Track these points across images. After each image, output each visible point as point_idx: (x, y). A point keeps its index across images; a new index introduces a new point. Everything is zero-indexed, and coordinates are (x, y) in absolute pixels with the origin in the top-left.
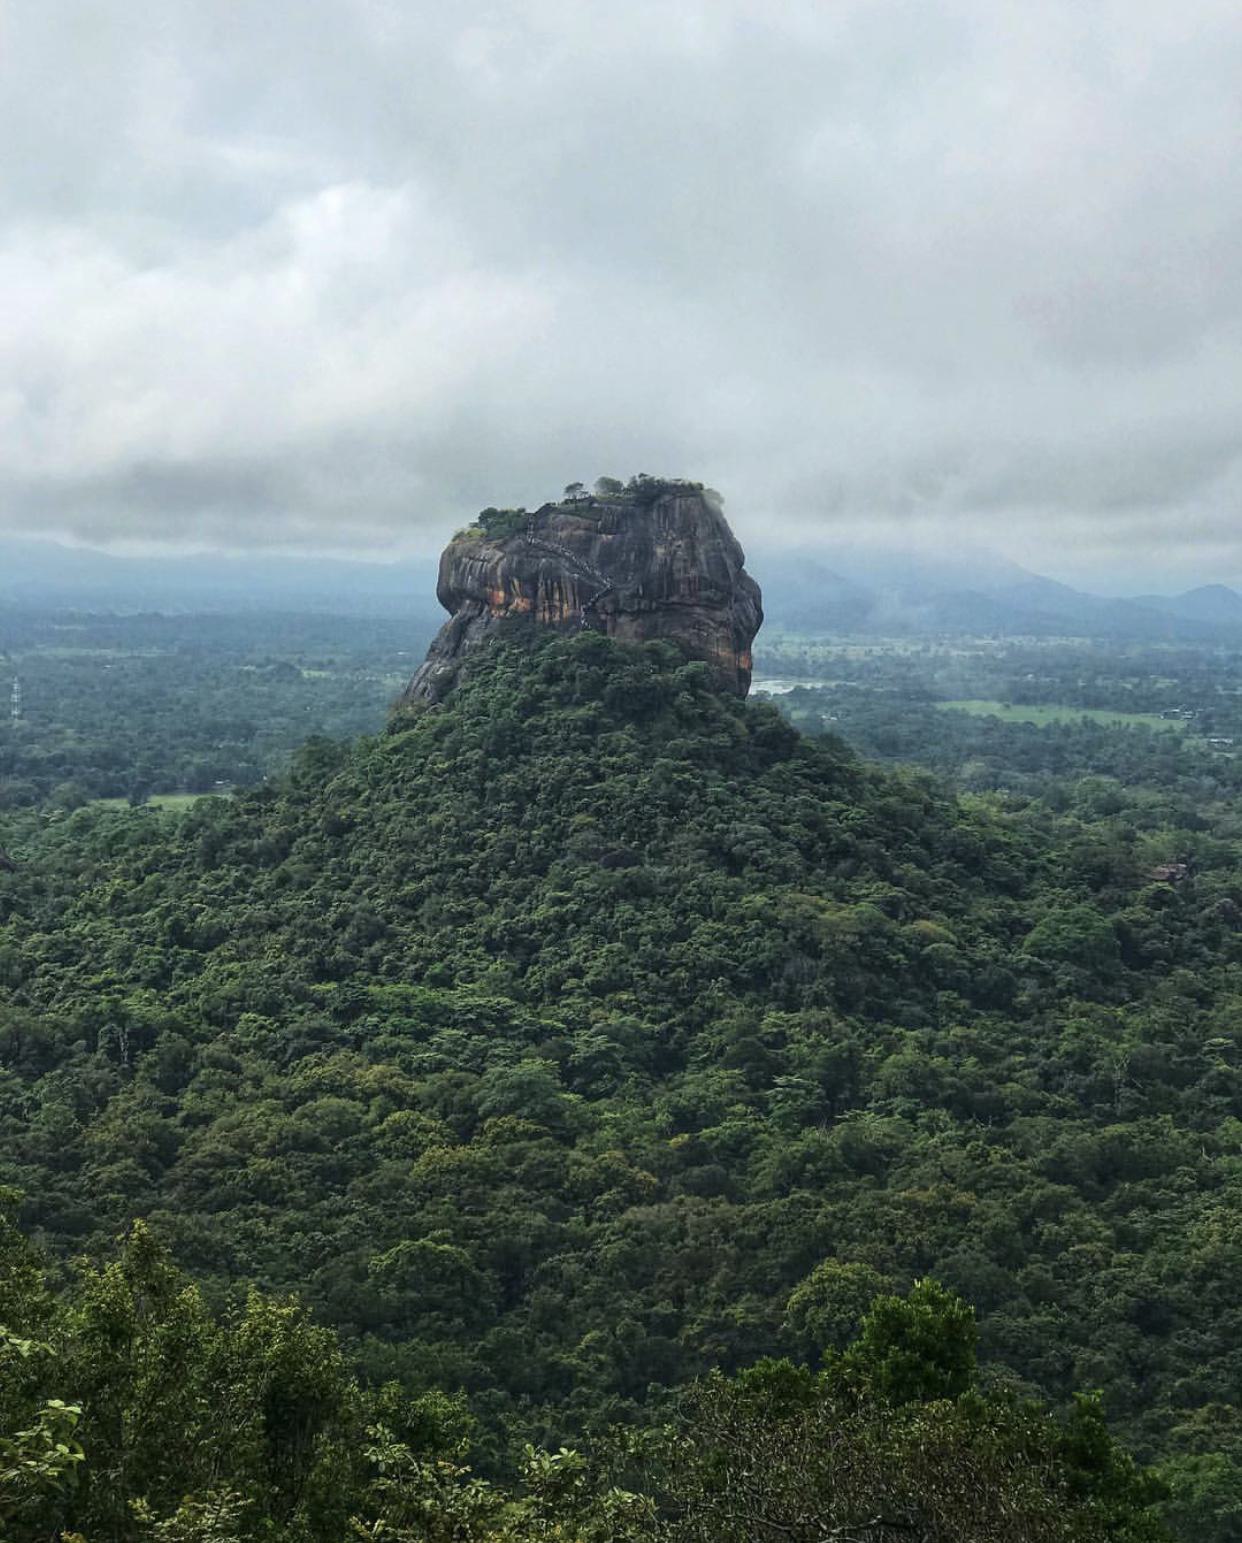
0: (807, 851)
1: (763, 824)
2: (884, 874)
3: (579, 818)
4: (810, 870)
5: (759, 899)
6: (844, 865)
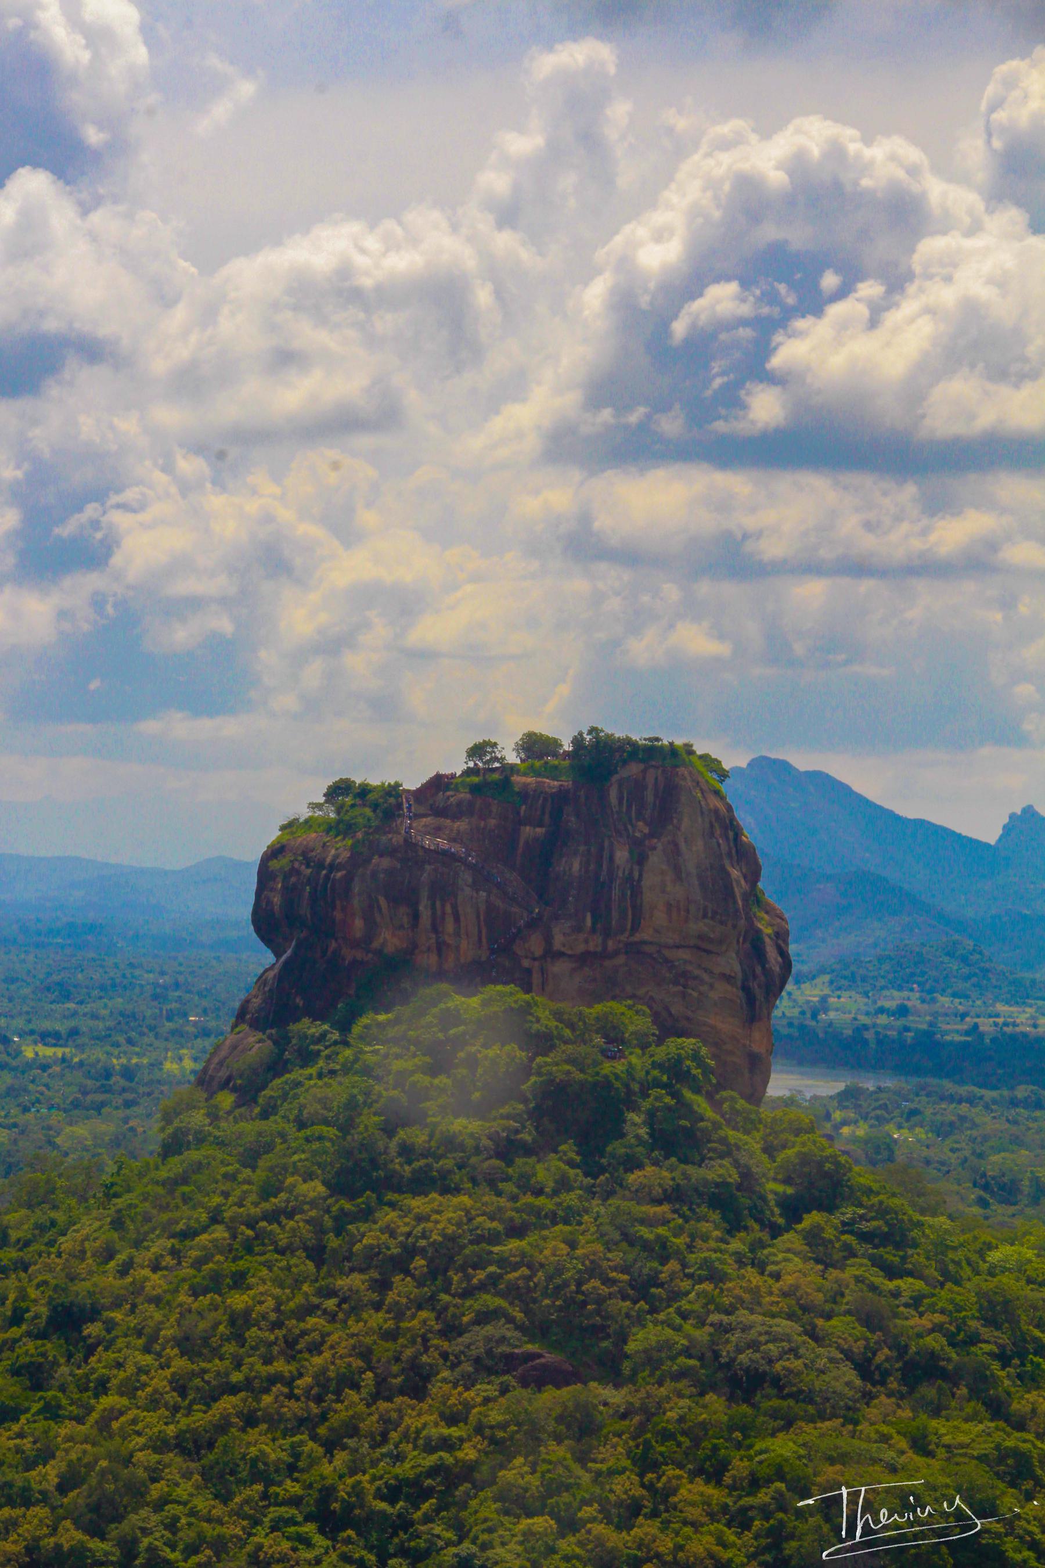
0: (864, 1367)
1: (790, 1316)
2: (997, 1409)
4: (868, 1397)
5: (782, 1447)
6: (929, 1391)
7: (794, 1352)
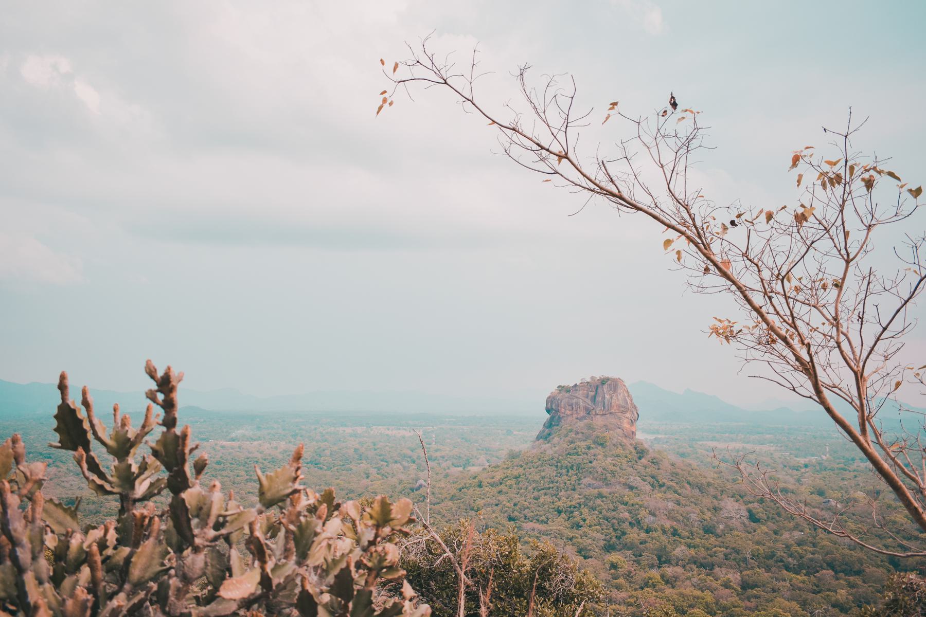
0: (652, 485)
6: (663, 489)
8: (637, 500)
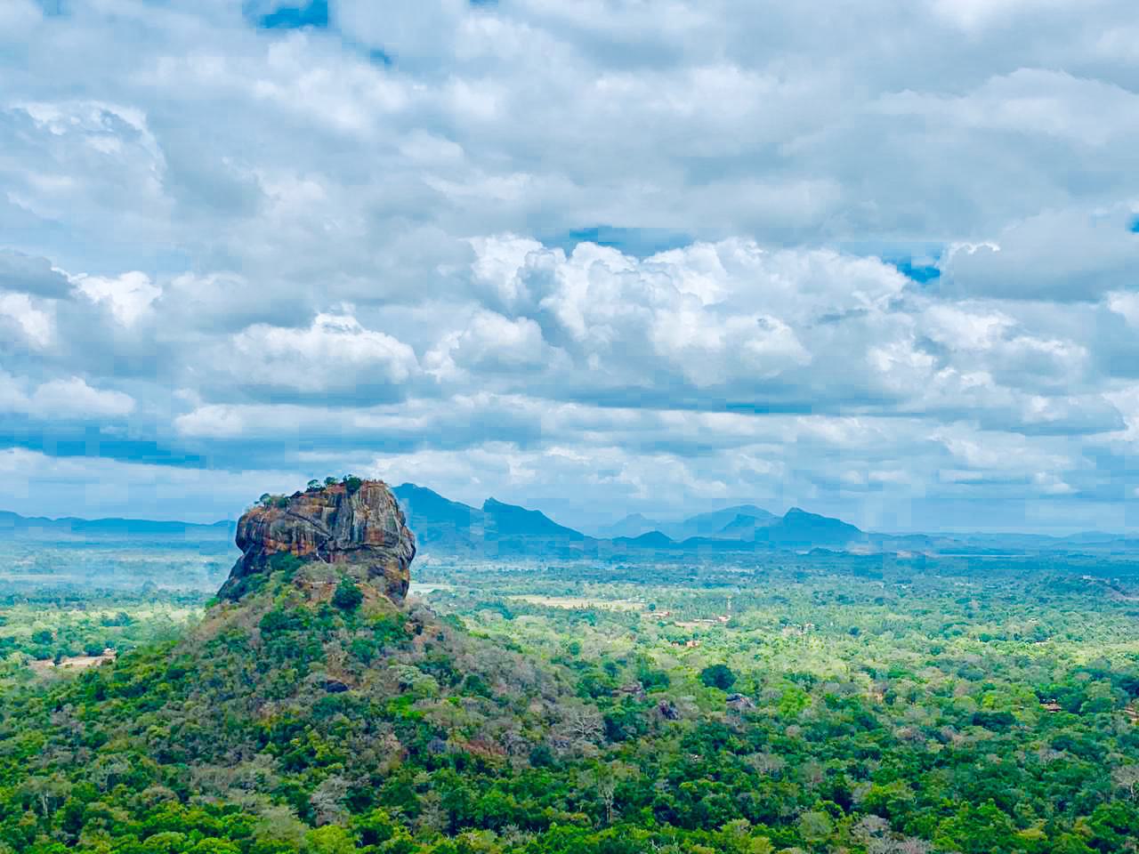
3: (317, 664)
7: (416, 676)
8: (410, 709)
